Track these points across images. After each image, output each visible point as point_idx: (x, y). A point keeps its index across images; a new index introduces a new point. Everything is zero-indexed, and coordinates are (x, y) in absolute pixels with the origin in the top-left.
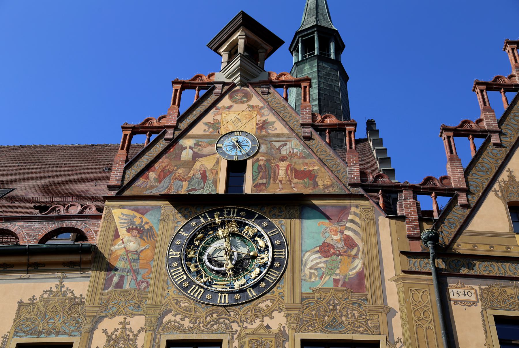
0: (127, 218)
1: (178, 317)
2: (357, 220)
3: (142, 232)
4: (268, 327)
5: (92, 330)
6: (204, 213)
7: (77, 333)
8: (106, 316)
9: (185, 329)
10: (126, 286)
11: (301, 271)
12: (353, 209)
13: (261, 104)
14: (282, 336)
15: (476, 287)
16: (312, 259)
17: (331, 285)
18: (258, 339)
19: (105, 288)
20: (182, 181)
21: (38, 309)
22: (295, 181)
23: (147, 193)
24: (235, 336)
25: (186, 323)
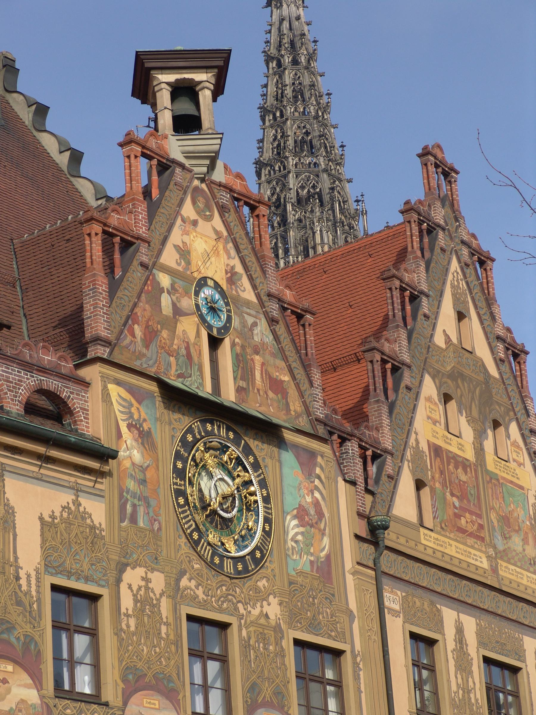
0: (124, 403)
1: (193, 583)
2: (323, 477)
3: (145, 437)
4: (267, 616)
5: (119, 581)
6: (197, 422)
7: (103, 583)
8: (127, 565)
9: (200, 602)
10: (141, 524)
11: (285, 542)
12: (319, 459)
13: (225, 233)
14: (277, 629)
15: (399, 593)
16: (293, 526)
17: (308, 568)
18: (261, 630)
19: (122, 520)
20: (170, 355)
21: (62, 535)
22: (271, 394)
23: (136, 365)
24: (243, 622)
25: (200, 592)
